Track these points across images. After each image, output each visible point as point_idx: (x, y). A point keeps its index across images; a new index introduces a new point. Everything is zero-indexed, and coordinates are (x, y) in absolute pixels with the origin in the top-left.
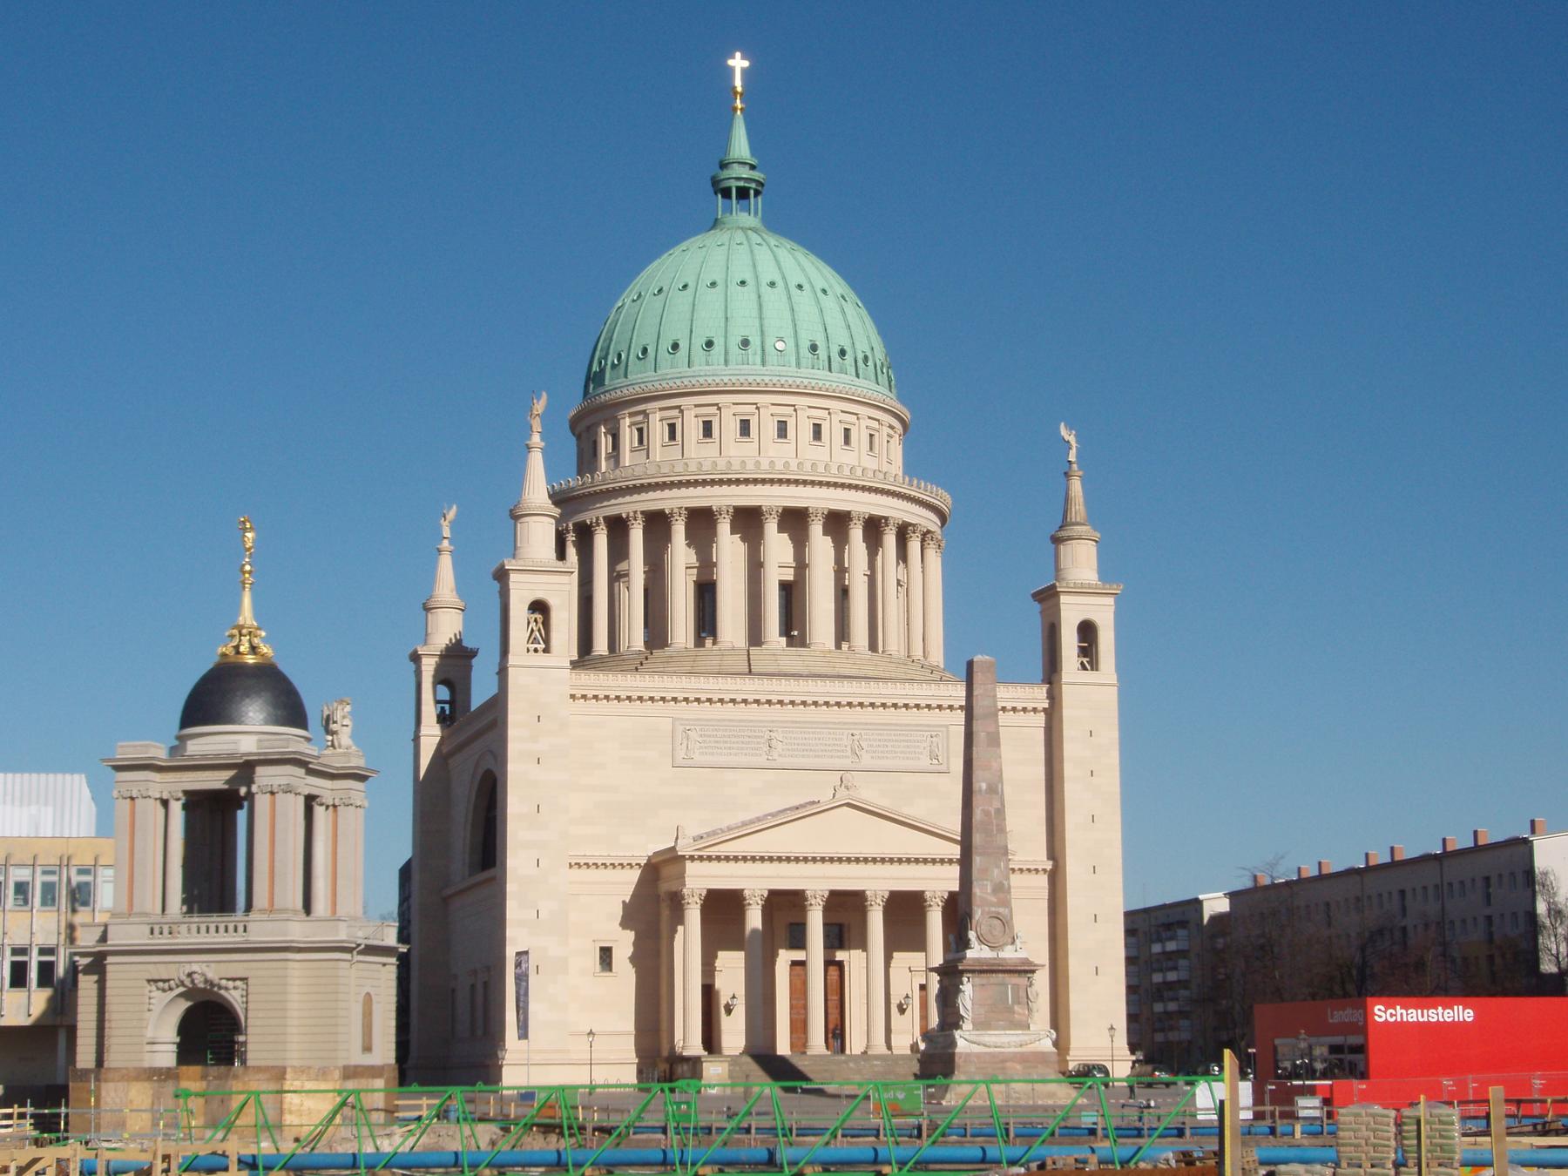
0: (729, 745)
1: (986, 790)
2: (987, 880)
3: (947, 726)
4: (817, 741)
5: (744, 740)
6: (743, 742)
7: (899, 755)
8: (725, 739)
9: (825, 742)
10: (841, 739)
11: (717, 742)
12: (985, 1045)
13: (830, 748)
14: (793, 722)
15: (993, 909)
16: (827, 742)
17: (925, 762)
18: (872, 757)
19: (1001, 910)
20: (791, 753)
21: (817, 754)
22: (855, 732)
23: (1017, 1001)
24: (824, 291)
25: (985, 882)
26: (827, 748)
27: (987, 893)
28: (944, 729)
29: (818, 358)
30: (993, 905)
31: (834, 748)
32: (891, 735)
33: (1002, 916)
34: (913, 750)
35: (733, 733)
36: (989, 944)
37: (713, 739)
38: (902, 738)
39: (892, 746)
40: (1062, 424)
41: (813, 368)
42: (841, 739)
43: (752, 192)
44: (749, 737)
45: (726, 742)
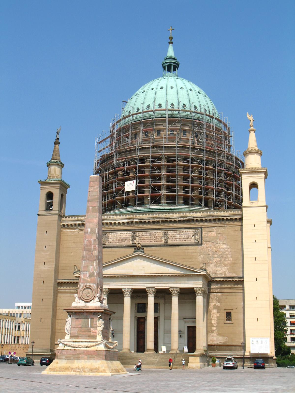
1: (90, 231)
2: (87, 271)
3: (201, 228)
11: (113, 238)
12: (71, 346)
13: (156, 238)
15: (88, 284)
16: (155, 236)
19: (92, 285)
23: (92, 326)
24: (182, 88)
25: (86, 272)
27: (86, 277)
28: (200, 229)
30: (88, 282)
33: (92, 287)
34: (188, 237)
36: (85, 300)
40: (248, 113)
43: (172, 66)
44: (126, 236)
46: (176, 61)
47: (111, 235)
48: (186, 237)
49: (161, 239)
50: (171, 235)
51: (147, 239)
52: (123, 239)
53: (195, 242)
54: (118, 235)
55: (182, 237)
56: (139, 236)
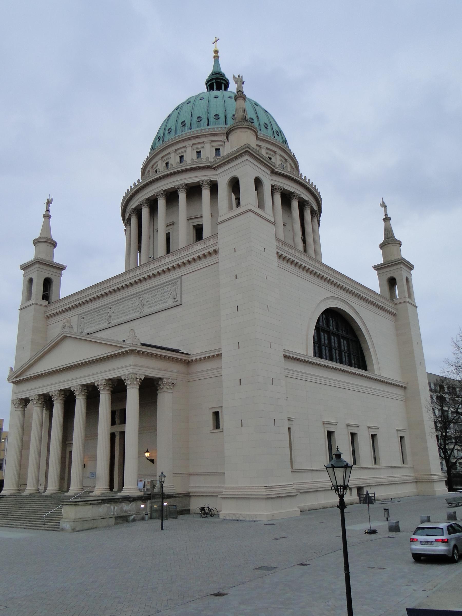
4: (127, 307)
13: (131, 309)
17: (170, 303)
22: (139, 297)
28: (179, 279)
29: (185, 127)
41: (182, 132)
43: (215, 84)
44: (102, 314)
46: (220, 76)
48: (163, 298)
49: (136, 309)
53: (174, 302)
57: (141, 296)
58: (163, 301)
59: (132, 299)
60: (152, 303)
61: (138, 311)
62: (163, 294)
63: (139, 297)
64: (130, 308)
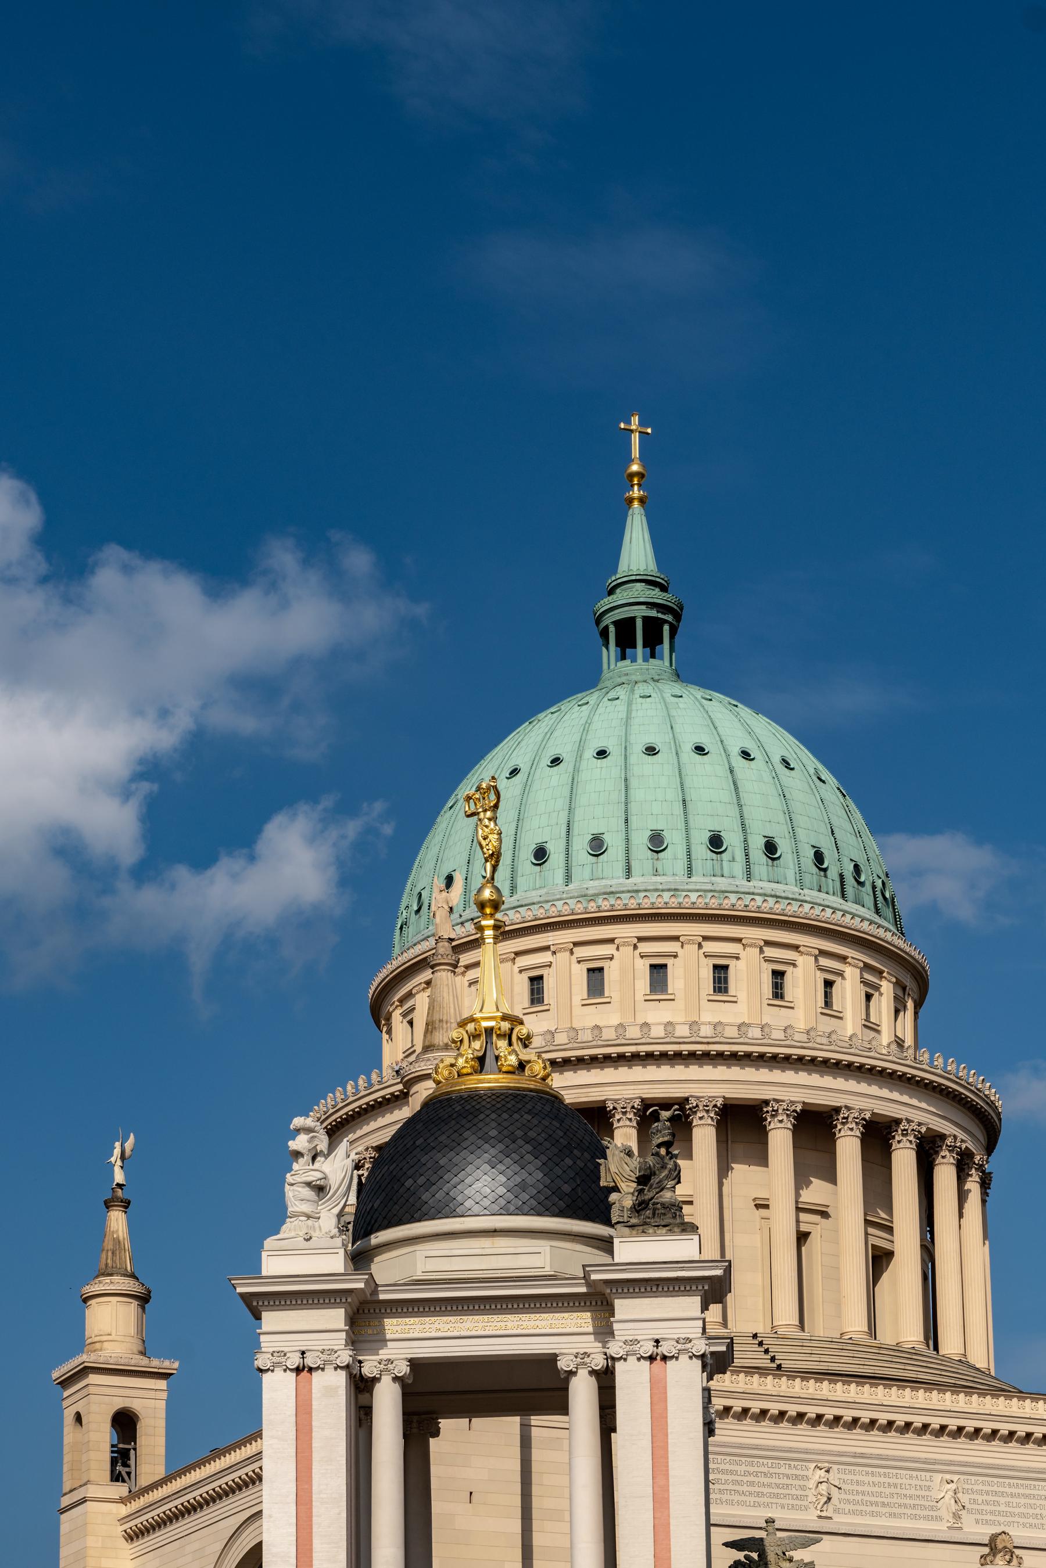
0: (757, 1489)
4: (893, 1490)
5: (778, 1481)
6: (778, 1486)
7: (1016, 1519)
8: (751, 1479)
9: (904, 1492)
10: (929, 1488)
14: (855, 1456)
16: (908, 1492)
18: (977, 1521)
20: (852, 1507)
21: (894, 1510)
22: (948, 1477)
26: (908, 1501)
31: (917, 1502)
32: (1003, 1485)
35: (762, 1469)
37: (731, 1478)
38: (1021, 1491)
39: (1008, 1504)
42: (929, 1488)
44: (788, 1477)
45: (752, 1484)
47: (722, 1467)
48: (1031, 1511)
49: (932, 1508)
50: (972, 1496)
51: (876, 1504)
52: (776, 1491)
54: (751, 1469)
55: (1017, 1510)
56: (843, 1486)
57: (955, 1478)
58: (1031, 1520)
59: (914, 1473)
60: (991, 1513)
61: (939, 1519)
62: (1032, 1502)
63: (948, 1477)
64: (905, 1496)
